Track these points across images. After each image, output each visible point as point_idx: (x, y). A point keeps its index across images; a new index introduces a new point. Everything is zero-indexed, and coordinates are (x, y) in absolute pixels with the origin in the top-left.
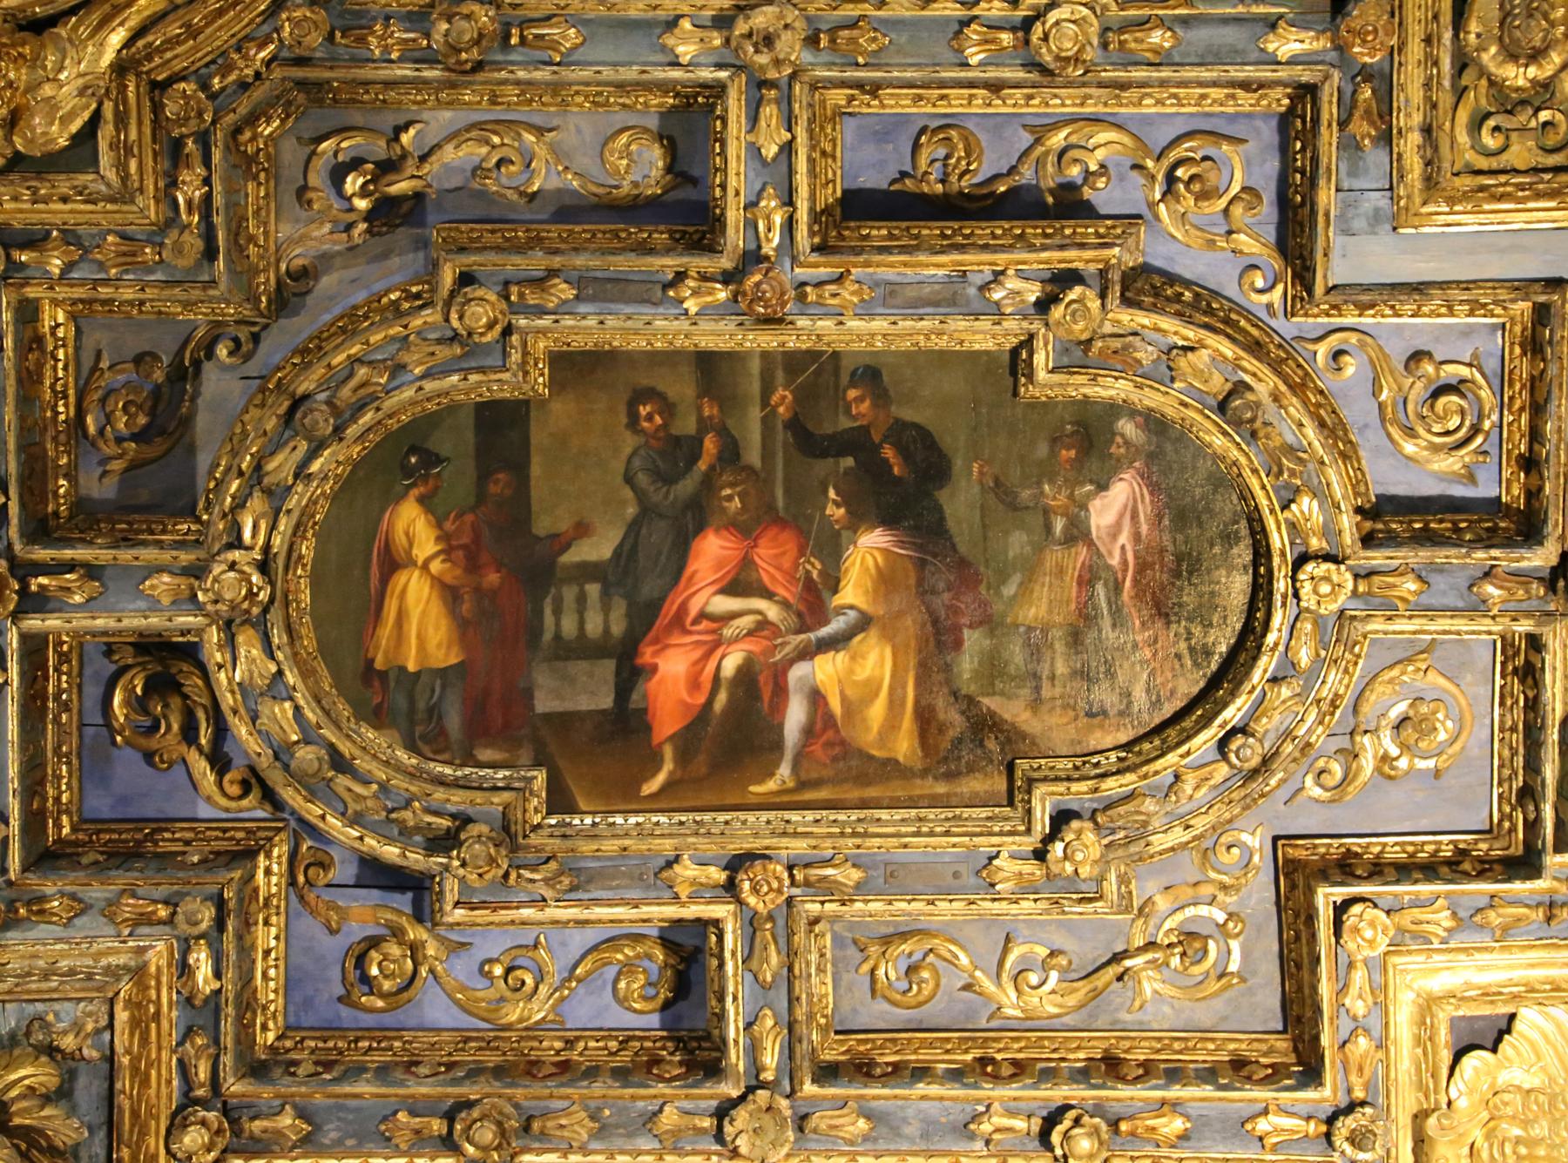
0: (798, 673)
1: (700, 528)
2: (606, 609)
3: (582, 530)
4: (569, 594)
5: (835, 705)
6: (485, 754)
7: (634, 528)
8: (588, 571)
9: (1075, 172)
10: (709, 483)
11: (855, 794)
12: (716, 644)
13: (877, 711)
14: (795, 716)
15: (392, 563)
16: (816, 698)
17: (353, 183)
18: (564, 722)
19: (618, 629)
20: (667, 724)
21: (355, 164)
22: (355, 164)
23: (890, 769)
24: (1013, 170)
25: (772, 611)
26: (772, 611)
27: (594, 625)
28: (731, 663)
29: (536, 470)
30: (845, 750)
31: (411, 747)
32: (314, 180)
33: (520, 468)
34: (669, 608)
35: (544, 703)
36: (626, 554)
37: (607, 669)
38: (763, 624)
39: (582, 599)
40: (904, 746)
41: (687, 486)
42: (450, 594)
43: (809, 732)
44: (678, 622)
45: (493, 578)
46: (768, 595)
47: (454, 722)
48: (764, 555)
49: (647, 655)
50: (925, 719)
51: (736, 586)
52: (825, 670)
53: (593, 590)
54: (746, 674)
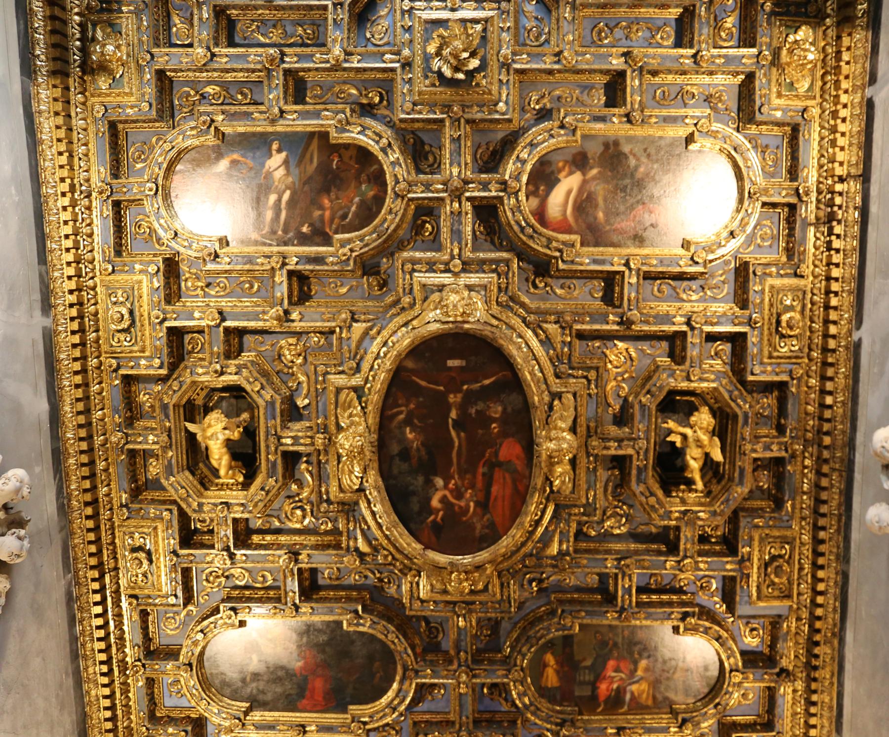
0: (629, 688)
1: (609, 659)
2: (589, 674)
3: (584, 659)
4: (582, 673)
5: (636, 694)
6: (565, 704)
7: (596, 659)
8: (586, 668)
9: (682, 584)
10: (611, 650)
11: (640, 712)
12: (612, 683)
13: (644, 696)
14: (628, 697)
15: (545, 665)
16: (632, 693)
17: (534, 584)
18: (580, 698)
19: (592, 678)
20: (602, 698)
21: (533, 580)
22: (533, 580)
23: (647, 707)
24: (670, 583)
25: (623, 676)
26: (623, 676)
27: (587, 678)
28: (615, 686)
29: (575, 647)
30: (638, 703)
31: (550, 702)
32: (525, 583)
33: (571, 646)
34: (603, 675)
35: (577, 694)
36: (593, 665)
37: (590, 687)
38: (621, 679)
39: (585, 673)
40: (650, 702)
41: (606, 650)
42: (557, 672)
43: (631, 700)
44: (604, 678)
45: (566, 669)
46: (621, 672)
47: (558, 697)
48: (622, 665)
49: (598, 684)
50: (654, 698)
51: (617, 670)
52: (634, 687)
53: (587, 671)
54: (618, 688)
